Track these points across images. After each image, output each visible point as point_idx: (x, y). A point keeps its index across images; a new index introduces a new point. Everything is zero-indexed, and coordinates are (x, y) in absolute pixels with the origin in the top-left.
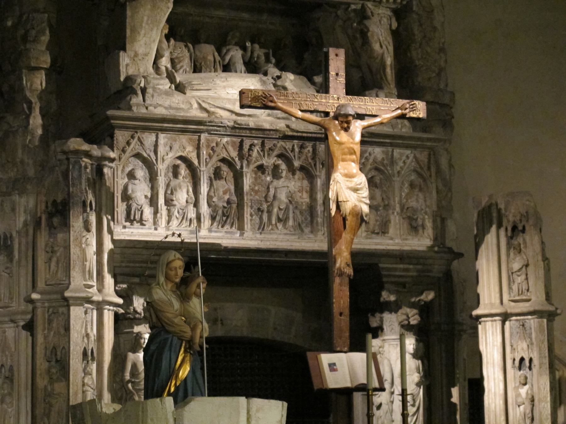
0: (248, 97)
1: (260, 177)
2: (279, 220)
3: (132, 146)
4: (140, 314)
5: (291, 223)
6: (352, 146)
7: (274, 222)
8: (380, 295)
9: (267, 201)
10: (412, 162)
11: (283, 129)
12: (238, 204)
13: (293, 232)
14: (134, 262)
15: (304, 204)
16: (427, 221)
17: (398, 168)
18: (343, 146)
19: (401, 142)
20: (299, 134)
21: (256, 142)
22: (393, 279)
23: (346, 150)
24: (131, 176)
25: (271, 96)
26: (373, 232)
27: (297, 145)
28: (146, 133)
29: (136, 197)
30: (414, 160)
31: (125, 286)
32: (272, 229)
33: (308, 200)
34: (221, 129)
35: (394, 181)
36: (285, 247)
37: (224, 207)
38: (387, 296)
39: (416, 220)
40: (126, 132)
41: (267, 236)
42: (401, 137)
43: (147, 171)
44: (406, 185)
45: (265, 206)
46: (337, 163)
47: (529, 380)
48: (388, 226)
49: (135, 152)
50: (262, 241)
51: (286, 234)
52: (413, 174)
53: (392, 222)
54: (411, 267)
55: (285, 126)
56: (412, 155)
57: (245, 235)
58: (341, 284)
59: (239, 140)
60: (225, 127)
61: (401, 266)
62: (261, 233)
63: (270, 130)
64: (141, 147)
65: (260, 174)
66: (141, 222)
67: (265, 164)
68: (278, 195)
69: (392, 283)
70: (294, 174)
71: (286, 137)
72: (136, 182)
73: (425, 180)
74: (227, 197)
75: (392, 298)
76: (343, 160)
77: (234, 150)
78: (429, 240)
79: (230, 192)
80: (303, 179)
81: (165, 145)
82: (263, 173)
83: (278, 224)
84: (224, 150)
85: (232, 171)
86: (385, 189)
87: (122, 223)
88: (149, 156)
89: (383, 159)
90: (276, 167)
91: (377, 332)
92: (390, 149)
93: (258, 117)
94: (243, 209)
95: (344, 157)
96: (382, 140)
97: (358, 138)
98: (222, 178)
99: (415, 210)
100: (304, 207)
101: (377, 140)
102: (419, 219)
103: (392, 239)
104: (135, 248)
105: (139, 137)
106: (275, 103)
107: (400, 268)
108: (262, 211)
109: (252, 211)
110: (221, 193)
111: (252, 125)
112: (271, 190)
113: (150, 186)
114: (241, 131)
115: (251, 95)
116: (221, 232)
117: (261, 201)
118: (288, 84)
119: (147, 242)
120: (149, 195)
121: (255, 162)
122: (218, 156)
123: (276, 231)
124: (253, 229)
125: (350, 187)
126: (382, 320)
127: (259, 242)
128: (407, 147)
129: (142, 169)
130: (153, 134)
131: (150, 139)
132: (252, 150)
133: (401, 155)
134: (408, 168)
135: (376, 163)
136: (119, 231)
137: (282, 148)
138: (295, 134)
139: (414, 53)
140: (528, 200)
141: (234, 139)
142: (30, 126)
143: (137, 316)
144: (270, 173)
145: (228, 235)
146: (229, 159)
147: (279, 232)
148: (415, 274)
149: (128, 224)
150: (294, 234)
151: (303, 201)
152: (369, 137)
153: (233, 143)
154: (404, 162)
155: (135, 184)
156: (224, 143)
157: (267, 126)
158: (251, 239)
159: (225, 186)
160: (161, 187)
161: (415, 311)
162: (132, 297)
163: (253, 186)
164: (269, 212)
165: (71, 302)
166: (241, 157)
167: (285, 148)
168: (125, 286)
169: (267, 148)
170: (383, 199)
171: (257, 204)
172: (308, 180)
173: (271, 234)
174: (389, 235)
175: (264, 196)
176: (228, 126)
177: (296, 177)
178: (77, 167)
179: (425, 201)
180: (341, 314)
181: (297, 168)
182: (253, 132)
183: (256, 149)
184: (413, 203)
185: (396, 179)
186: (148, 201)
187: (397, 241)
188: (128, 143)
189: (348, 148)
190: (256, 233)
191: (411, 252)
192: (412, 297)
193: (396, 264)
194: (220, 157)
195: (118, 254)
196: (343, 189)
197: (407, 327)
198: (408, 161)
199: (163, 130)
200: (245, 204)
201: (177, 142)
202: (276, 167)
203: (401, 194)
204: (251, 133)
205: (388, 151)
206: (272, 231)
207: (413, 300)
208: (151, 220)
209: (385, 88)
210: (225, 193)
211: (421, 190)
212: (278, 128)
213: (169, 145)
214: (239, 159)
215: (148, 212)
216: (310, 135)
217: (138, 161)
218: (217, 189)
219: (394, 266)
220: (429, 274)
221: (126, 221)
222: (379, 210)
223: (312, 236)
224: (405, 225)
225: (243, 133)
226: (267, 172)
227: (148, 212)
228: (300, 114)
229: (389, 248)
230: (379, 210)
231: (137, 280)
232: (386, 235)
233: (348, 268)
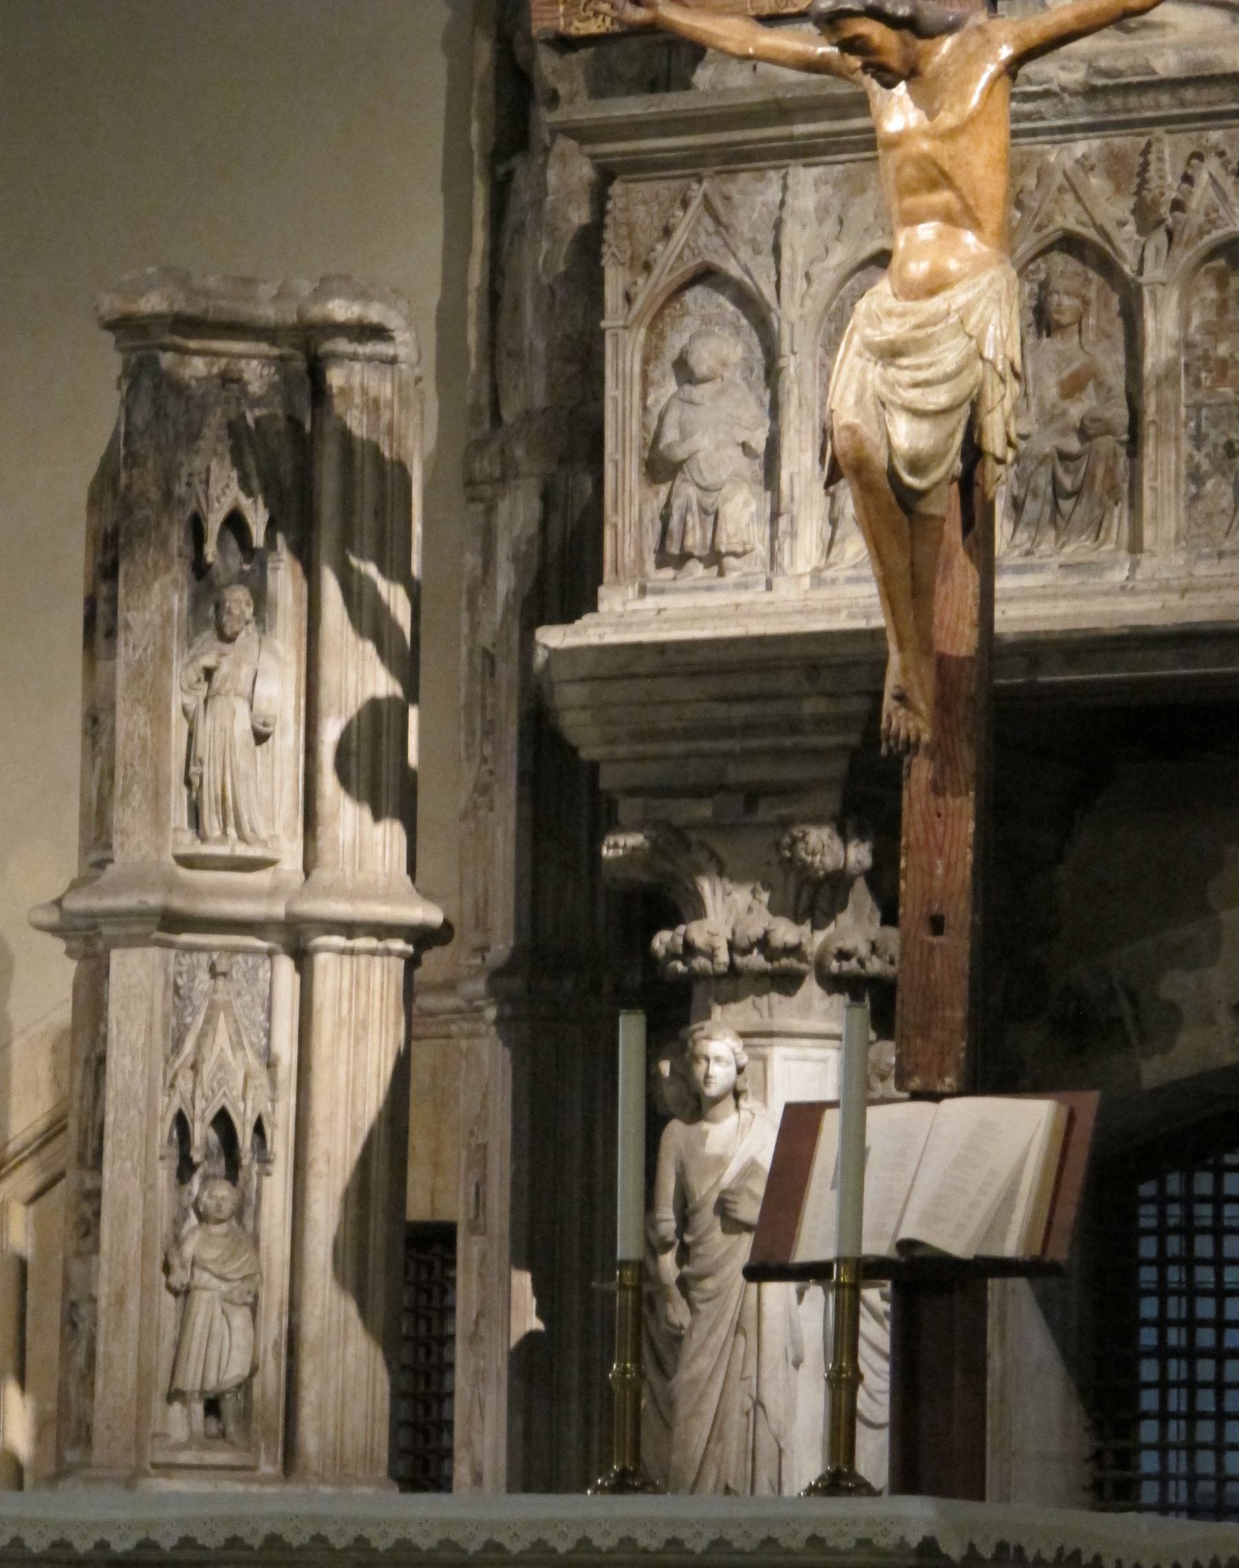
3: (680, 236)
4: (711, 955)
6: (925, 146)
14: (655, 735)
21: (1215, 136)
23: (910, 171)
24: (684, 370)
28: (743, 177)
29: (692, 456)
31: (635, 840)
34: (1043, 105)
37: (1064, 456)
40: (661, 185)
43: (755, 339)
49: (692, 263)
50: (1184, 592)
58: (937, 789)
59: (1143, 141)
60: (1047, 94)
64: (717, 241)
66: (714, 558)
72: (700, 392)
74: (1076, 411)
77: (1118, 189)
79: (1100, 385)
81: (823, 211)
84: (1069, 198)
85: (1113, 288)
87: (643, 574)
88: (747, 272)
95: (909, 202)
98: (1061, 327)
104: (633, 676)
105: (705, 197)
109: (1198, 457)
110: (1052, 391)
111: (1167, 64)
113: (767, 398)
114: (1133, 100)
116: (1041, 568)
119: (660, 648)
120: (759, 441)
121: (1202, 233)
122: (1039, 228)
127: (1173, 600)
129: (737, 330)
130: (772, 174)
131: (760, 199)
136: (618, 608)
141: (1121, 141)
142: (550, 198)
143: (700, 963)
145: (1073, 581)
146: (1090, 233)
149: (668, 573)
153: (1114, 164)
155: (692, 403)
156: (1069, 164)
159: (1069, 361)
160: (794, 400)
162: (694, 884)
165: (107, 930)
166: (1146, 216)
168: (635, 840)
176: (1064, 89)
178: (146, 383)
180: (937, 925)
182: (1189, 94)
186: (757, 466)
188: (667, 232)
194: (1052, 231)
195: (583, 708)
199: (806, 151)
201: (870, 194)
204: (1182, 104)
208: (762, 550)
210: (1072, 388)
213: (836, 208)
215: (742, 513)
217: (722, 299)
218: (1038, 378)
221: (660, 565)
225: (1142, 108)
227: (742, 513)
231: (704, 810)
233: (902, 712)
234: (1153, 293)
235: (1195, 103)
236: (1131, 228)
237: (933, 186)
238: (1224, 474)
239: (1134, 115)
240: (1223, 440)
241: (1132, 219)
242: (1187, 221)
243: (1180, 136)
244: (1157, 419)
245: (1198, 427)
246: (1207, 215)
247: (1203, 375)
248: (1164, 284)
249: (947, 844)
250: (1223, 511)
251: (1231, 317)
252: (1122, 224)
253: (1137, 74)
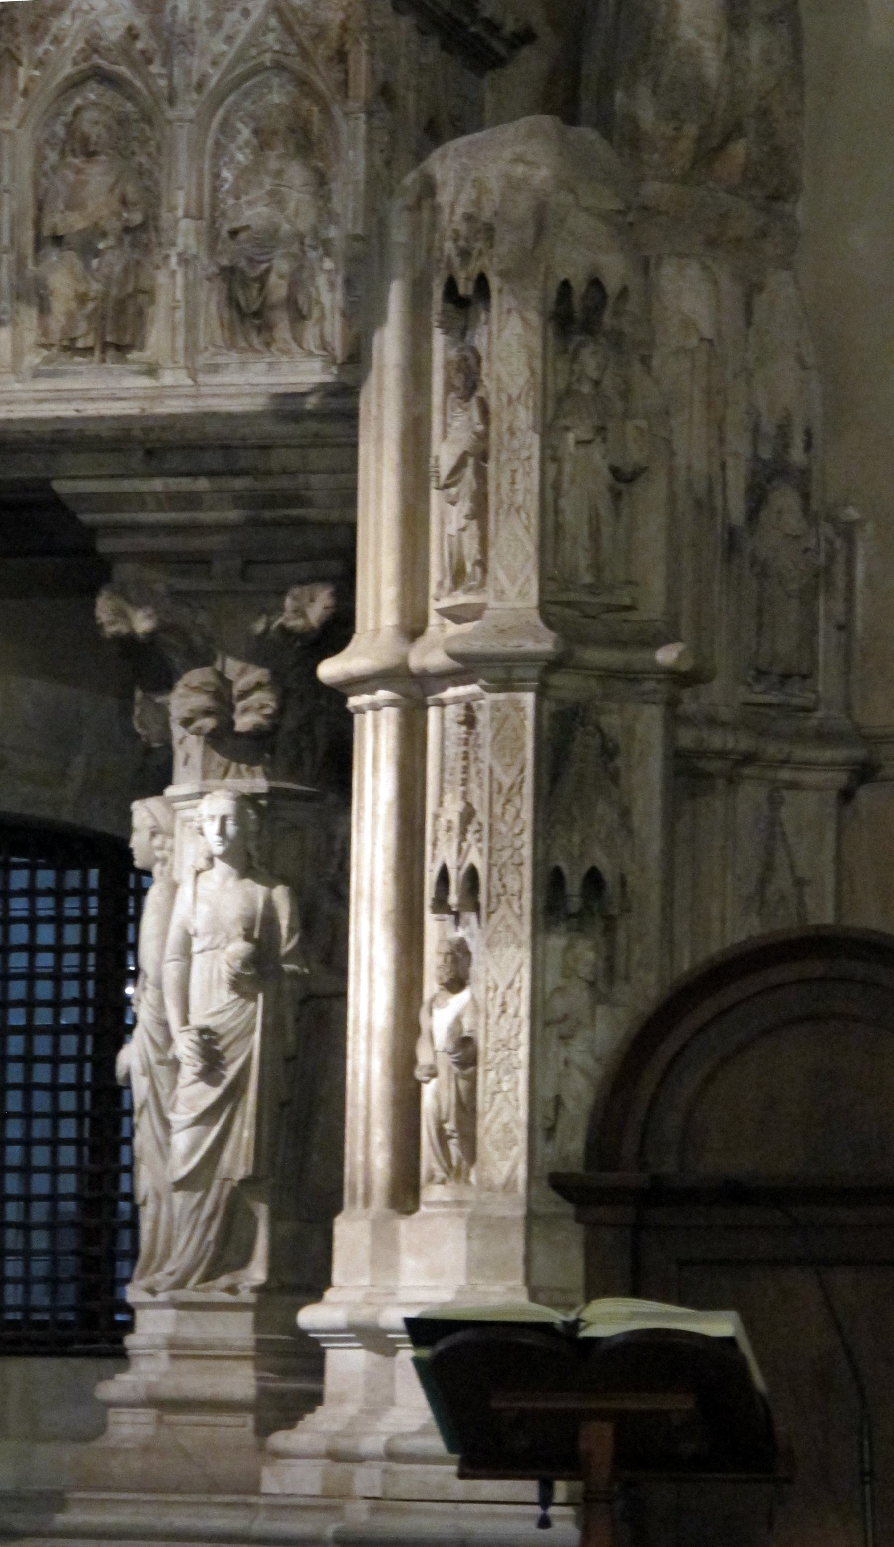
10: (262, 28)
16: (322, 281)
22: (145, 542)
26: (71, 348)
30: (273, 22)
35: (170, 122)
39: (262, 279)
44: (246, 133)
47: (476, 969)
48: (140, 313)
52: (275, 81)
53: (163, 299)
54: (203, 484)
61: (158, 484)
78: (317, 365)
89: (132, 34)
99: (269, 239)
102: (273, 279)
103: (152, 371)
107: (154, 494)
134: (240, 58)
135: (96, 50)
140: (519, 159)
148: (233, 515)
161: (257, 674)
174: (147, 355)
184: (254, 213)
193: (134, 475)
197: (223, 740)
203: (217, 176)
220: (295, 512)
222: (98, 253)
224: (213, 308)
229: (91, 409)
230: (98, 253)
232: (133, 355)
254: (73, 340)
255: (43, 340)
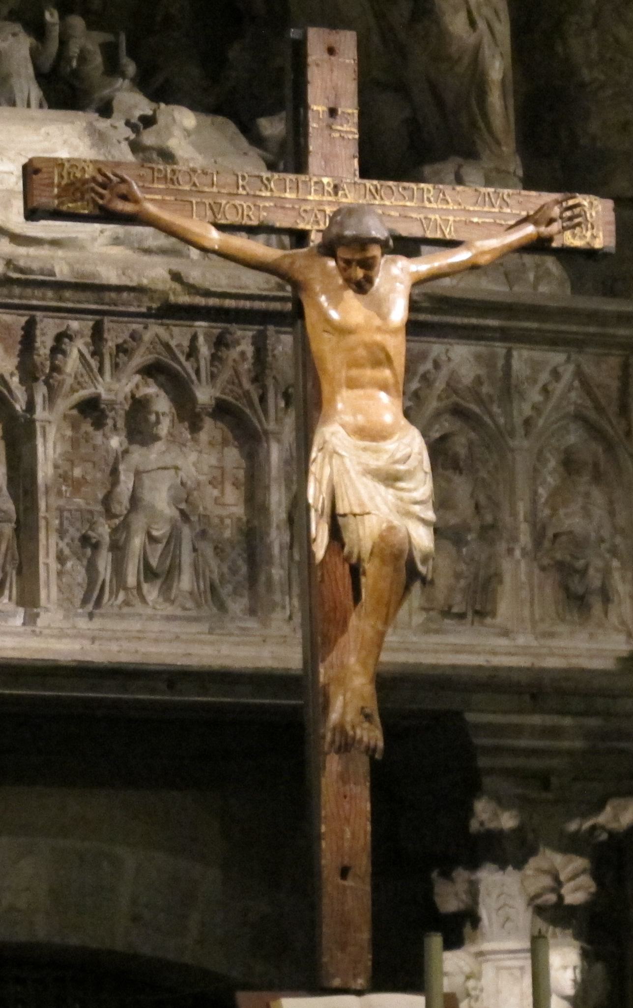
0: (51, 185)
1: (87, 438)
2: (149, 573)
5: (186, 581)
6: (378, 337)
7: (131, 580)
8: (469, 812)
9: (109, 514)
10: (570, 388)
11: (160, 286)
12: (18, 522)
13: (193, 613)
15: (228, 521)
16: (616, 575)
17: (527, 410)
18: (352, 339)
19: (535, 325)
20: (212, 302)
21: (75, 325)
22: (509, 762)
23: (361, 352)
25: (123, 181)
26: (447, 613)
27: (207, 336)
30: (576, 383)
32: (126, 603)
33: (239, 510)
35: (512, 450)
36: (169, 660)
38: (492, 815)
41: (110, 624)
42: (535, 311)
44: (552, 463)
45: (104, 530)
46: (334, 393)
48: (494, 591)
50: (93, 640)
51: (169, 618)
52: (572, 427)
53: (507, 579)
54: (567, 721)
55: (168, 277)
56: (571, 368)
57: (40, 622)
58: (344, 778)
59: (23, 320)
61: (536, 720)
62: (91, 616)
63: (119, 289)
65: (87, 427)
67: (105, 396)
68: (147, 496)
69: (508, 773)
70: (195, 428)
71: (169, 312)
73: (610, 447)
75: (508, 821)
76: (353, 384)
77: (6, 350)
80: (225, 443)
82: (99, 424)
83: (145, 587)
86: (483, 474)
89: (478, 380)
90: (139, 406)
91: (458, 928)
92: (500, 348)
93: (82, 248)
94: (35, 539)
95: (354, 372)
96: (474, 321)
97: (399, 313)
99: (578, 543)
100: (227, 534)
101: (458, 320)
102: (591, 571)
103: (505, 633)
106: (136, 201)
107: (533, 727)
108: (96, 547)
109: (62, 545)
111: (62, 272)
112: (122, 477)
114: (29, 291)
115: (61, 177)
117: (91, 512)
118: (177, 144)
121: (73, 390)
123: (139, 608)
124: (65, 602)
125: (371, 469)
126: (473, 891)
127: (86, 643)
128: (555, 341)
132: (64, 353)
133: (536, 366)
134: (557, 408)
135: (455, 392)
137: (160, 348)
138: (200, 301)
139: (576, 46)
144: (121, 423)
147: (149, 611)
148: (579, 744)
150: (196, 619)
151: (224, 512)
152: (432, 311)
154: (545, 390)
157: (111, 276)
158: (61, 635)
161: (580, 862)
163: (66, 466)
164: (118, 549)
166: (28, 373)
167: (167, 346)
169: (110, 344)
170: (477, 507)
171: (78, 524)
172: (240, 447)
173: (122, 617)
174: (499, 620)
175: (100, 496)
177: (203, 436)
179: (612, 513)
180: (344, 872)
181: (204, 408)
182: (68, 294)
183: (77, 349)
184: (572, 520)
185: (519, 442)
187: (521, 640)
189: (369, 346)
190: (77, 615)
191: (567, 674)
192: (570, 817)
193: (520, 711)
196: (353, 474)
198: (559, 388)
200: (42, 523)
202: (139, 406)
203: (535, 493)
204: (61, 299)
205: (493, 356)
206: (125, 610)
207: (573, 826)
209: (485, 155)
211: (597, 477)
212: (145, 282)
214: (22, 381)
216: (248, 304)
219: (515, 719)
220: (623, 745)
222: (467, 543)
223: (252, 624)
224: (548, 590)
225: (33, 297)
226: (110, 422)
228: (214, 237)
230: (467, 543)
232: (488, 620)
233: (366, 725)
234: (44, 428)
235: (68, 300)
236: (16, 379)
237: (377, 363)
238: (78, 559)
239: (24, 302)
240: (78, 535)
241: (16, 372)
242: (64, 380)
243: (50, 320)
244: (48, 516)
245: (61, 524)
246: (76, 377)
247: (64, 488)
248: (50, 422)
249: (353, 816)
250: (79, 584)
251: (83, 451)
252: (12, 375)
253: (42, 274)
254: (450, 607)
255: (426, 605)
